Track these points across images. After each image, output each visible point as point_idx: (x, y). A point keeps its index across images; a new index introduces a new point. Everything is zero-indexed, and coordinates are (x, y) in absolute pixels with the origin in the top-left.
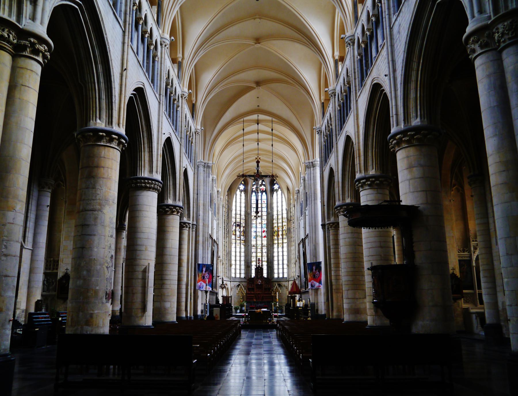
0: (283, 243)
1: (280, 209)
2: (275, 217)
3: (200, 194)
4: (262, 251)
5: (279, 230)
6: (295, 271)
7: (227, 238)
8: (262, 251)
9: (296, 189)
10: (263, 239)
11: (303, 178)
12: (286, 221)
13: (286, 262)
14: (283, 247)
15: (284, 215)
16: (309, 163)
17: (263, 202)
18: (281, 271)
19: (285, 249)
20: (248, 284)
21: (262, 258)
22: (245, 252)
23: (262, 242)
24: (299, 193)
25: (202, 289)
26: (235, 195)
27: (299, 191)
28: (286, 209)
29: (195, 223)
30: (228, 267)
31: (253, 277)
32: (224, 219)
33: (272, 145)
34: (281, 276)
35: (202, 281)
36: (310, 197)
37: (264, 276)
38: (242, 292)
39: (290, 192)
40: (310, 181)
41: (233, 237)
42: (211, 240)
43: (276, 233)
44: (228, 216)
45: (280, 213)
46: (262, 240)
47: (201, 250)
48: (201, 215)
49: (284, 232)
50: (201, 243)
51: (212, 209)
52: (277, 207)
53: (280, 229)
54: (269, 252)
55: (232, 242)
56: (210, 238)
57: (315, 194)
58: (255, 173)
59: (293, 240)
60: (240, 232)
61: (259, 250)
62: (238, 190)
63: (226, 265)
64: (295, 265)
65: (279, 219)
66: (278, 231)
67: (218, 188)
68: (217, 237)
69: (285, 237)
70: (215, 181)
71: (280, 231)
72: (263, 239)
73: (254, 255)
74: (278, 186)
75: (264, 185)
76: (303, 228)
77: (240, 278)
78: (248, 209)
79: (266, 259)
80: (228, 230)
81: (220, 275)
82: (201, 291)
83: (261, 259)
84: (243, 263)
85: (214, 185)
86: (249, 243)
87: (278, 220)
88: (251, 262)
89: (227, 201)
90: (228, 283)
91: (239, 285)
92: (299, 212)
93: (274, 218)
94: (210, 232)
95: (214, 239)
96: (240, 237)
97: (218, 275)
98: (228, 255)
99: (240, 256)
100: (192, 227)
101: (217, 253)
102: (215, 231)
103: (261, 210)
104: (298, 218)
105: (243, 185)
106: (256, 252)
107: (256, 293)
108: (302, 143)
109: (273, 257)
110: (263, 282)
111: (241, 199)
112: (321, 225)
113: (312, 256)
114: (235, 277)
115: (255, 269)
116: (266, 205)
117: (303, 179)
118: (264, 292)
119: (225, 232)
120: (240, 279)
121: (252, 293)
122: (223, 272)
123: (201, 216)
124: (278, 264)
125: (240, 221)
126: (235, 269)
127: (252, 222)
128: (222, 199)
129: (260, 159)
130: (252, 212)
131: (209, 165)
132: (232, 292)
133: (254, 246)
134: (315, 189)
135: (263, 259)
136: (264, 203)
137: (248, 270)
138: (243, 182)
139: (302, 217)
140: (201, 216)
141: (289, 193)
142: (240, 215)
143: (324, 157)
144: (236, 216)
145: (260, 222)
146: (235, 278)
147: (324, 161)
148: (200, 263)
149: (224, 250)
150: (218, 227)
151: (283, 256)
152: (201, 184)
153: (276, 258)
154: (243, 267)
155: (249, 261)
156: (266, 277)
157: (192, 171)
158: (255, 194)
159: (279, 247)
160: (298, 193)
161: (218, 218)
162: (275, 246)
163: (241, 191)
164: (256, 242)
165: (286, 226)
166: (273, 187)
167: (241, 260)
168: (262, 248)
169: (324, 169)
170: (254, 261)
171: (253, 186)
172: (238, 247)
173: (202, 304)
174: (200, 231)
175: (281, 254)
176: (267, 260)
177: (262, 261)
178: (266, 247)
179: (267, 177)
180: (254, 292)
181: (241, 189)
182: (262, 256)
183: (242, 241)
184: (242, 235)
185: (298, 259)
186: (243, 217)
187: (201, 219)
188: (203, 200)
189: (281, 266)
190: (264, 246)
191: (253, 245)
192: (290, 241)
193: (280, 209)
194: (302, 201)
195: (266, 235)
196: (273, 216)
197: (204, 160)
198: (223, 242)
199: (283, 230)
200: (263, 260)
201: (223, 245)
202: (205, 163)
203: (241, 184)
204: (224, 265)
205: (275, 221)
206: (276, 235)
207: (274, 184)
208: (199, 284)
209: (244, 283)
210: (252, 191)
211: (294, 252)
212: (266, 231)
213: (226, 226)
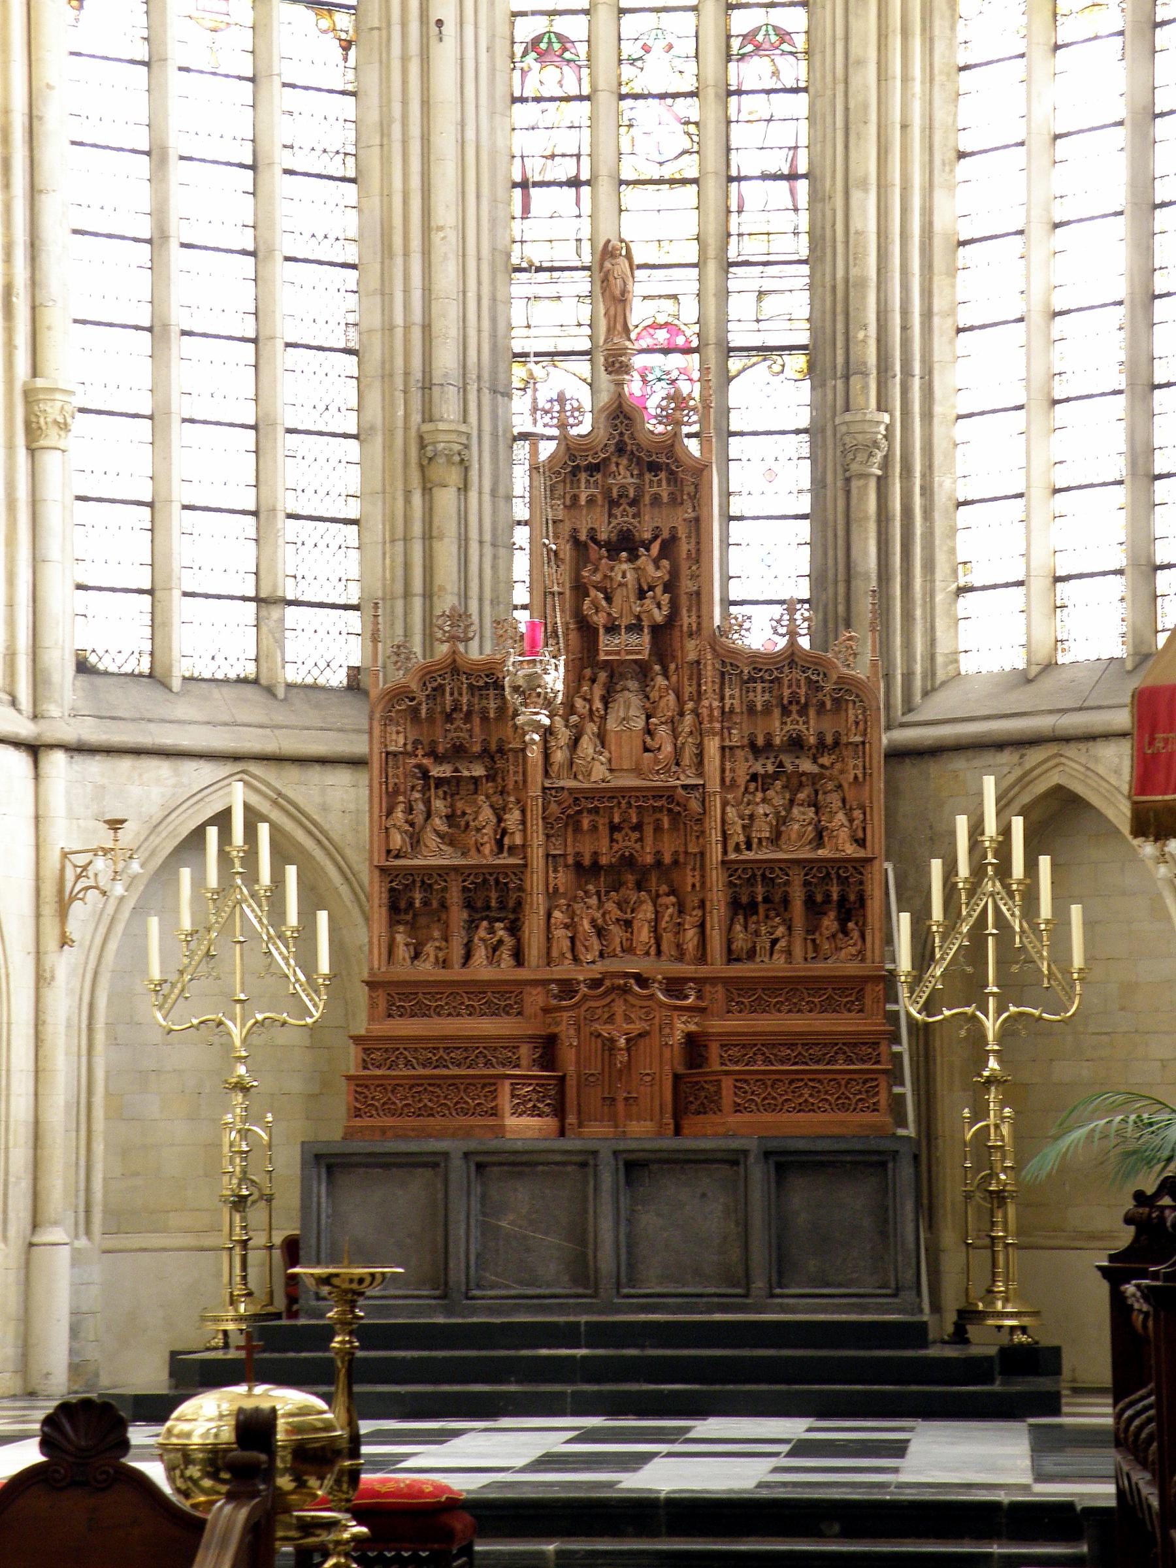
20: (390, 798)
79: (800, 304)
107: (565, 970)
110: (712, 746)
114: (156, 677)
118: (732, 957)
120: (252, 708)
121: (482, 969)
135: (740, 307)
137: (429, 537)
146: (159, 694)
155: (446, 359)
180: (518, 957)
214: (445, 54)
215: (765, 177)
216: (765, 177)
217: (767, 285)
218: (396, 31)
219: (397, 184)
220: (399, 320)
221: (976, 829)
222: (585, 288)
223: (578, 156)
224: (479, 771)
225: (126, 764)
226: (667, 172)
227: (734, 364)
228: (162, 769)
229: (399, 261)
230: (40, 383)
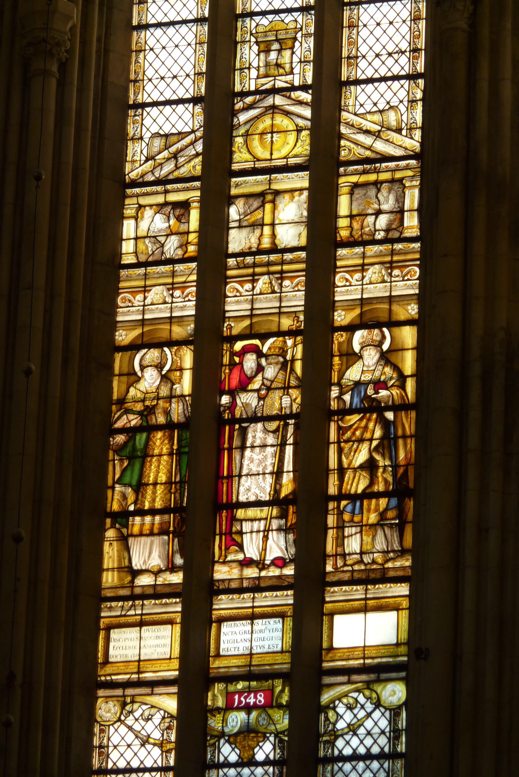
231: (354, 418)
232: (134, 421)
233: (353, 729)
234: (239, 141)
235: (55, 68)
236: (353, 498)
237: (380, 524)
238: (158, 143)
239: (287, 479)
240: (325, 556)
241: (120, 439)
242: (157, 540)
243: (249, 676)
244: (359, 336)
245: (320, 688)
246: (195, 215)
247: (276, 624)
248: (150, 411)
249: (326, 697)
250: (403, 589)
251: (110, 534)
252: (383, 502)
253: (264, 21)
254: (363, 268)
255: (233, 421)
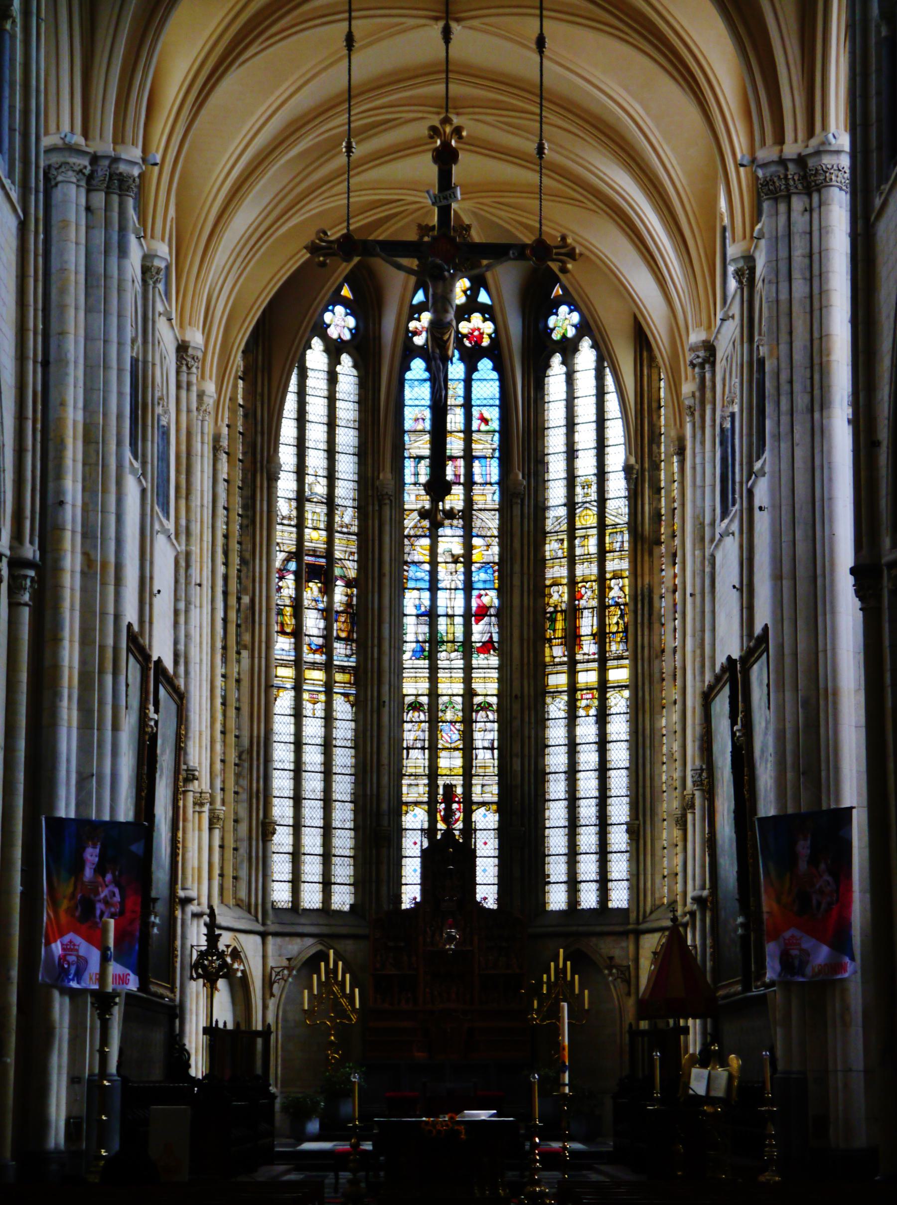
0: (603, 686)
1: (586, 465)
2: (556, 513)
3: (63, 362)
4: (467, 737)
5: (583, 603)
6: (679, 869)
7: (245, 654)
8: (472, 740)
9: (696, 337)
10: (478, 660)
11: (741, 264)
12: (626, 545)
13: (619, 811)
14: (602, 718)
15: (611, 505)
16: (782, 162)
17: (475, 425)
18: (588, 867)
19: (619, 728)
21: (468, 787)
22: (359, 743)
23: (468, 680)
24: (713, 365)
25: (74, 985)
26: (295, 371)
27: (710, 348)
28: (628, 469)
29: (30, 551)
30: (245, 844)
31: (406, 905)
32: (221, 527)
33: (541, 43)
34: (589, 898)
35: (77, 932)
36: (785, 387)
37: (479, 898)
38: (336, 1000)
39: (652, 359)
40: (784, 286)
41: (283, 645)
42: (132, 671)
43: (560, 625)
44: (250, 513)
45: (586, 494)
46: (468, 669)
47: (69, 728)
48: (69, 498)
49: (615, 620)
50: (70, 687)
51: (144, 464)
52: (571, 453)
53: (588, 599)
54: (517, 748)
55: (276, 682)
56: (129, 650)
57: (816, 368)
58: (424, 229)
59: (667, 667)
60: (328, 614)
61: (450, 735)
62: (317, 343)
63: (235, 830)
64: (677, 833)
65: (579, 533)
66: (573, 613)
67: (181, 326)
68: (176, 643)
69: (615, 648)
70: (162, 275)
71: (586, 613)
72: (478, 660)
73: (416, 761)
74: (575, 317)
75: (484, 310)
76: (735, 594)
77: (326, 908)
78: (378, 468)
79: (495, 789)
80: (246, 599)
81: (193, 894)
82: (67, 1000)
83: (459, 790)
84: (343, 815)
85: (160, 308)
86: (386, 688)
87: (572, 537)
88: (398, 807)
89: (245, 416)
90: (251, 945)
91: (321, 956)
92: (708, 490)
93: (550, 525)
94: (131, 615)
95: (155, 658)
96: (327, 648)
97: (181, 894)
98: (246, 765)
99: (328, 773)
100: (11, 576)
101: (180, 750)
102: (163, 606)
103: (462, 471)
104: (702, 525)
105: (346, 307)
106: (433, 750)
108: (742, 30)
109: (541, 776)
111: (332, 399)
112: (853, 571)
113: (790, 775)
115: (425, 855)
116: (496, 445)
117: (738, 274)
119: (232, 615)
122: (217, 871)
123: (74, 506)
124: (573, 825)
125: (330, 542)
126: (296, 855)
127: (407, 549)
128: (210, 402)
129: (460, 137)
130: (407, 488)
131: (122, 168)
132: (272, 1003)
133: (416, 707)
134: (816, 335)
135: (477, 790)
136: (484, 427)
138: (346, 292)
139: (726, 521)
140: (68, 508)
141: (650, 367)
142: (330, 502)
143: (879, 120)
144: (300, 510)
145: (458, 550)
147: (879, 148)
148: (62, 814)
149: (223, 733)
150: (182, 580)
151: (603, 769)
152: (70, 300)
153: (557, 788)
154: (344, 842)
155: (385, 806)
156: (494, 906)
157: (6, 208)
158: (428, 369)
159: (581, 712)
160: (702, 366)
161: (183, 522)
162: (557, 708)
163: (334, 350)
164: (433, 680)
165: (626, 581)
166: (541, 326)
167: (336, 796)
168: (468, 722)
169: (878, 202)
170: (416, 803)
171: (411, 319)
172: (313, 710)
173: (74, 1080)
174: (67, 604)
175: (588, 758)
176: (500, 795)
177: (469, 806)
178: (492, 716)
179: (507, 254)
181: (333, 333)
182: (468, 773)
183: (339, 677)
184: (339, 638)
185: (697, 793)
186: (347, 519)
187: (69, 526)
188: (80, 404)
189: (588, 839)
190: (486, 707)
191: (408, 700)
192: (651, 676)
193: (586, 465)
194: (733, 415)
195: (496, 638)
196: (541, 509)
197: (85, 134)
198: (219, 682)
199: (602, 609)
200: (476, 798)
201: (219, 701)
202: (95, 159)
203: (338, 299)
204: (223, 829)
205: (553, 547)
206: (559, 634)
207: (552, 308)
208: (57, 948)
209: (348, 946)
210: (410, 352)
211: (676, 746)
212: (492, 611)
213: (233, 573)
214: (386, 710)
215: (484, 748)
216: (484, 748)
217: (485, 782)
218: (369, 703)
219: (369, 750)
220: (369, 792)
221: (557, 966)
222: (426, 782)
223: (424, 740)
224: (402, 944)
225: (287, 939)
226: (453, 745)
227: (474, 807)
228: (298, 940)
229: (369, 774)
230: (267, 821)
231: (612, 608)
232: (551, 609)
233: (616, 705)
234: (577, 518)
235: (519, 501)
236: (613, 633)
237: (620, 642)
238: (555, 519)
239: (595, 627)
240: (606, 652)
241: (548, 615)
242: (560, 647)
243: (587, 689)
244: (613, 581)
245: (606, 692)
246: (565, 543)
247: (593, 672)
248: (556, 606)
249: (608, 695)
250: (626, 662)
251: (547, 645)
252: (621, 634)
253: (583, 479)
254: (613, 560)
255: (580, 609)
